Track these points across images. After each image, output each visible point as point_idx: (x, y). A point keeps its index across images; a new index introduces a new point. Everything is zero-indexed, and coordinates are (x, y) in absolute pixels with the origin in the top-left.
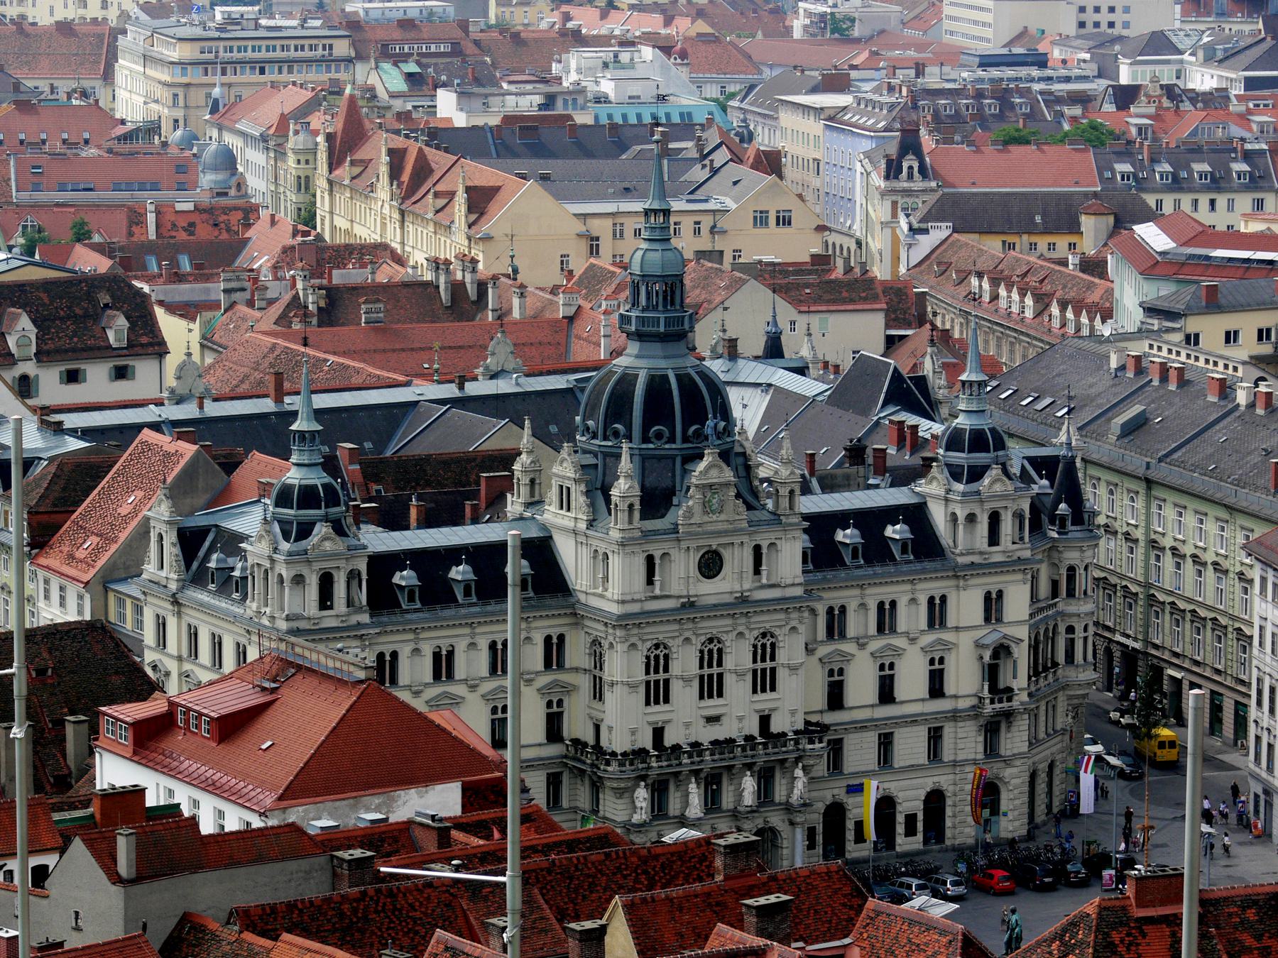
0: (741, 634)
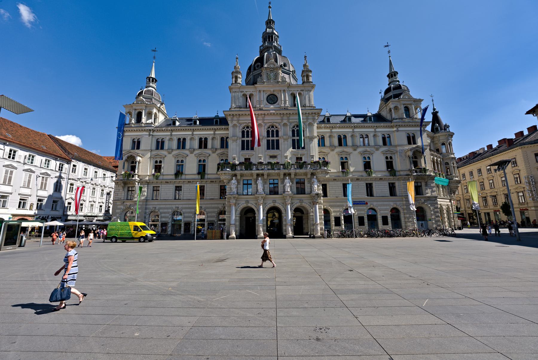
0: (285, 125)
